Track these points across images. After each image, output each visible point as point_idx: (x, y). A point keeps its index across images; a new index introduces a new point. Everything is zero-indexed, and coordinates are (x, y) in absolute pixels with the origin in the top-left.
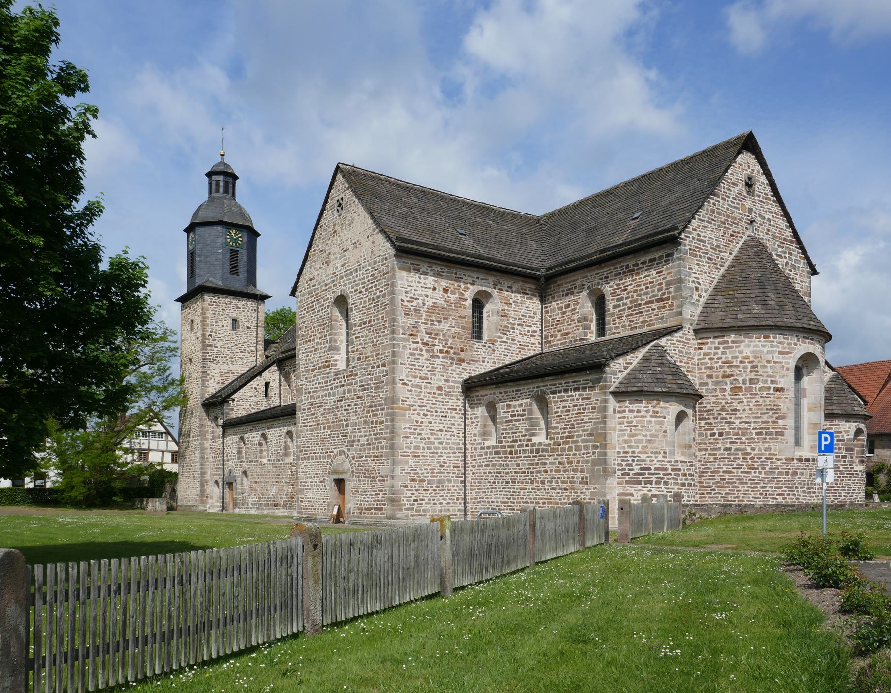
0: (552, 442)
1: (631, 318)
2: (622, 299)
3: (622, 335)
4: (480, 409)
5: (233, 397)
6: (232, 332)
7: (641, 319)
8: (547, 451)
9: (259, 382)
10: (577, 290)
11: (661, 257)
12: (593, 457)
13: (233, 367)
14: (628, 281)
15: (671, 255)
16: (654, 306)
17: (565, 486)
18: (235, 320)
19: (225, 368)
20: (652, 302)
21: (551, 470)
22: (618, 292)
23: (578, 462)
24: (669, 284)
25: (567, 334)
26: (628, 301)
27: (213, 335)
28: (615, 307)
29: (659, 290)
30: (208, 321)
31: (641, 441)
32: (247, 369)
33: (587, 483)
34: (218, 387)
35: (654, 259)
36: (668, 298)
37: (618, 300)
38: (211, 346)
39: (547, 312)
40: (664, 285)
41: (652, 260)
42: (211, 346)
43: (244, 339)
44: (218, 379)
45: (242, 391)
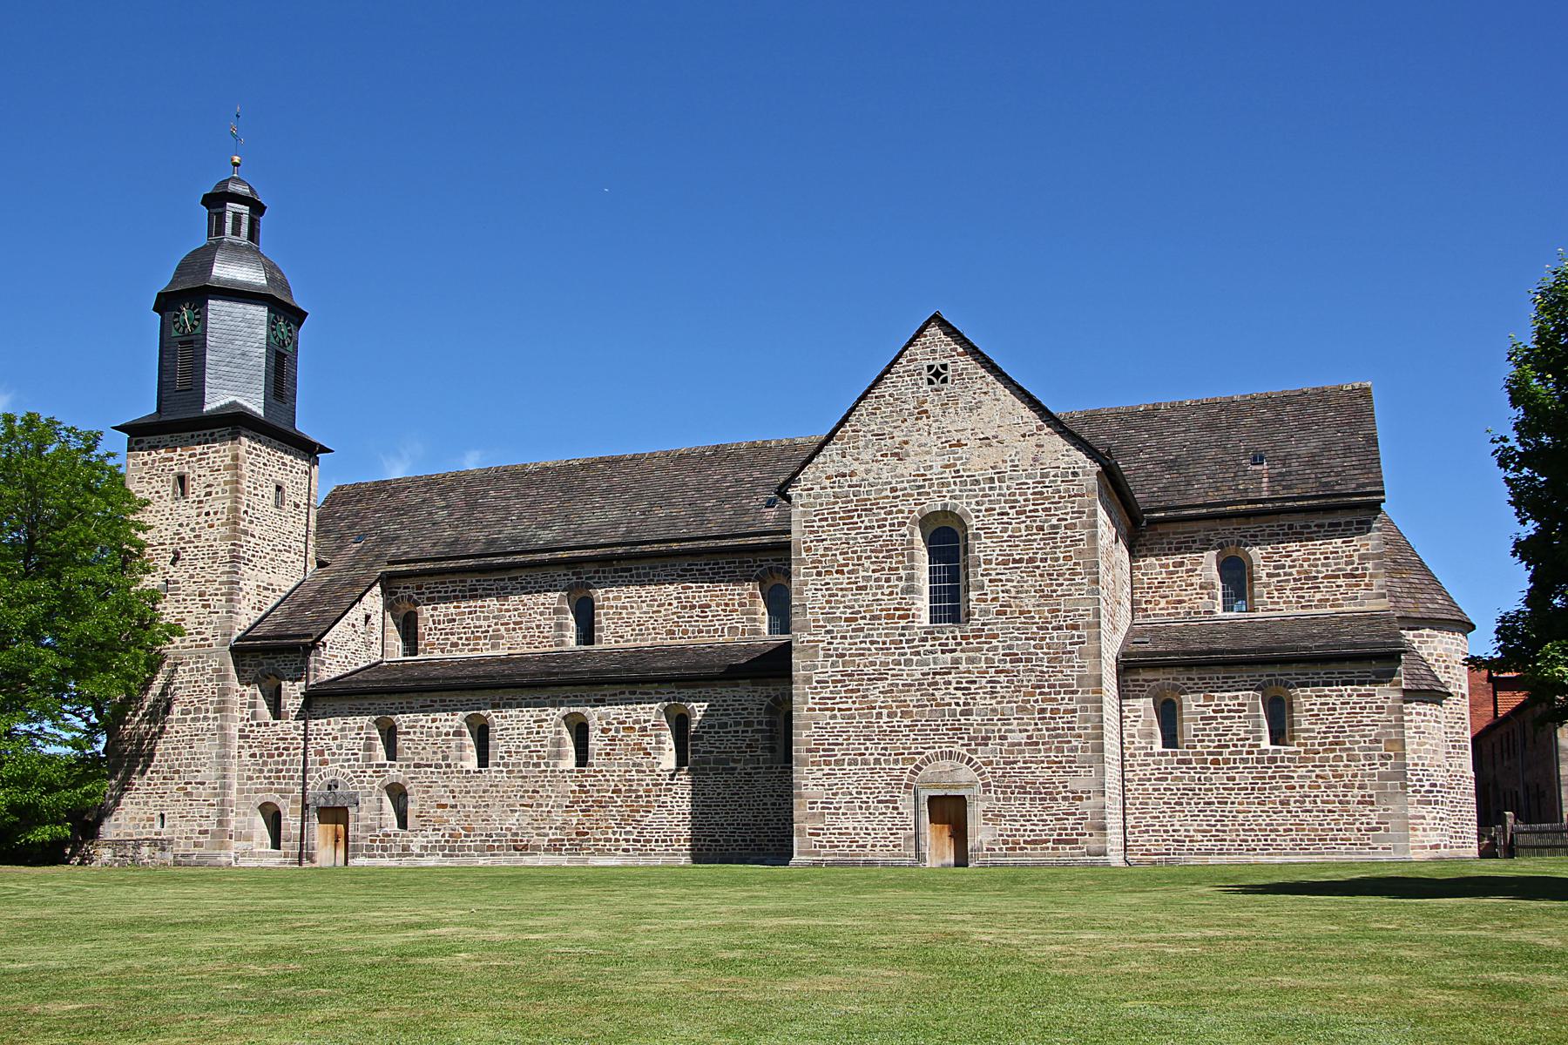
0: (1302, 749)
1: (1300, 593)
2: (1283, 567)
3: (1285, 613)
4: (1142, 700)
5: (324, 639)
6: (275, 510)
7: (1318, 596)
8: (1290, 760)
9: (356, 614)
10: (1197, 545)
11: (1349, 523)
12: (1382, 769)
13: (274, 579)
14: (1293, 546)
15: (1369, 523)
16: (1339, 581)
17: (1330, 807)
18: (279, 488)
19: (264, 578)
20: (1338, 577)
21: (1302, 787)
22: (1276, 557)
23: (1354, 776)
24: (1362, 557)
25: (1180, 602)
26: (1294, 571)
27: (250, 511)
28: (1268, 575)
29: (1347, 564)
30: (245, 483)
31: (1427, 751)
32: (293, 585)
33: (1372, 803)
34: (256, 616)
35: (1339, 524)
36: (1364, 575)
37: (1276, 568)
38: (246, 533)
39: (1139, 568)
40: (1356, 559)
41: (1331, 525)
42: (246, 533)
43: (289, 527)
44: (254, 599)
45: (336, 627)
